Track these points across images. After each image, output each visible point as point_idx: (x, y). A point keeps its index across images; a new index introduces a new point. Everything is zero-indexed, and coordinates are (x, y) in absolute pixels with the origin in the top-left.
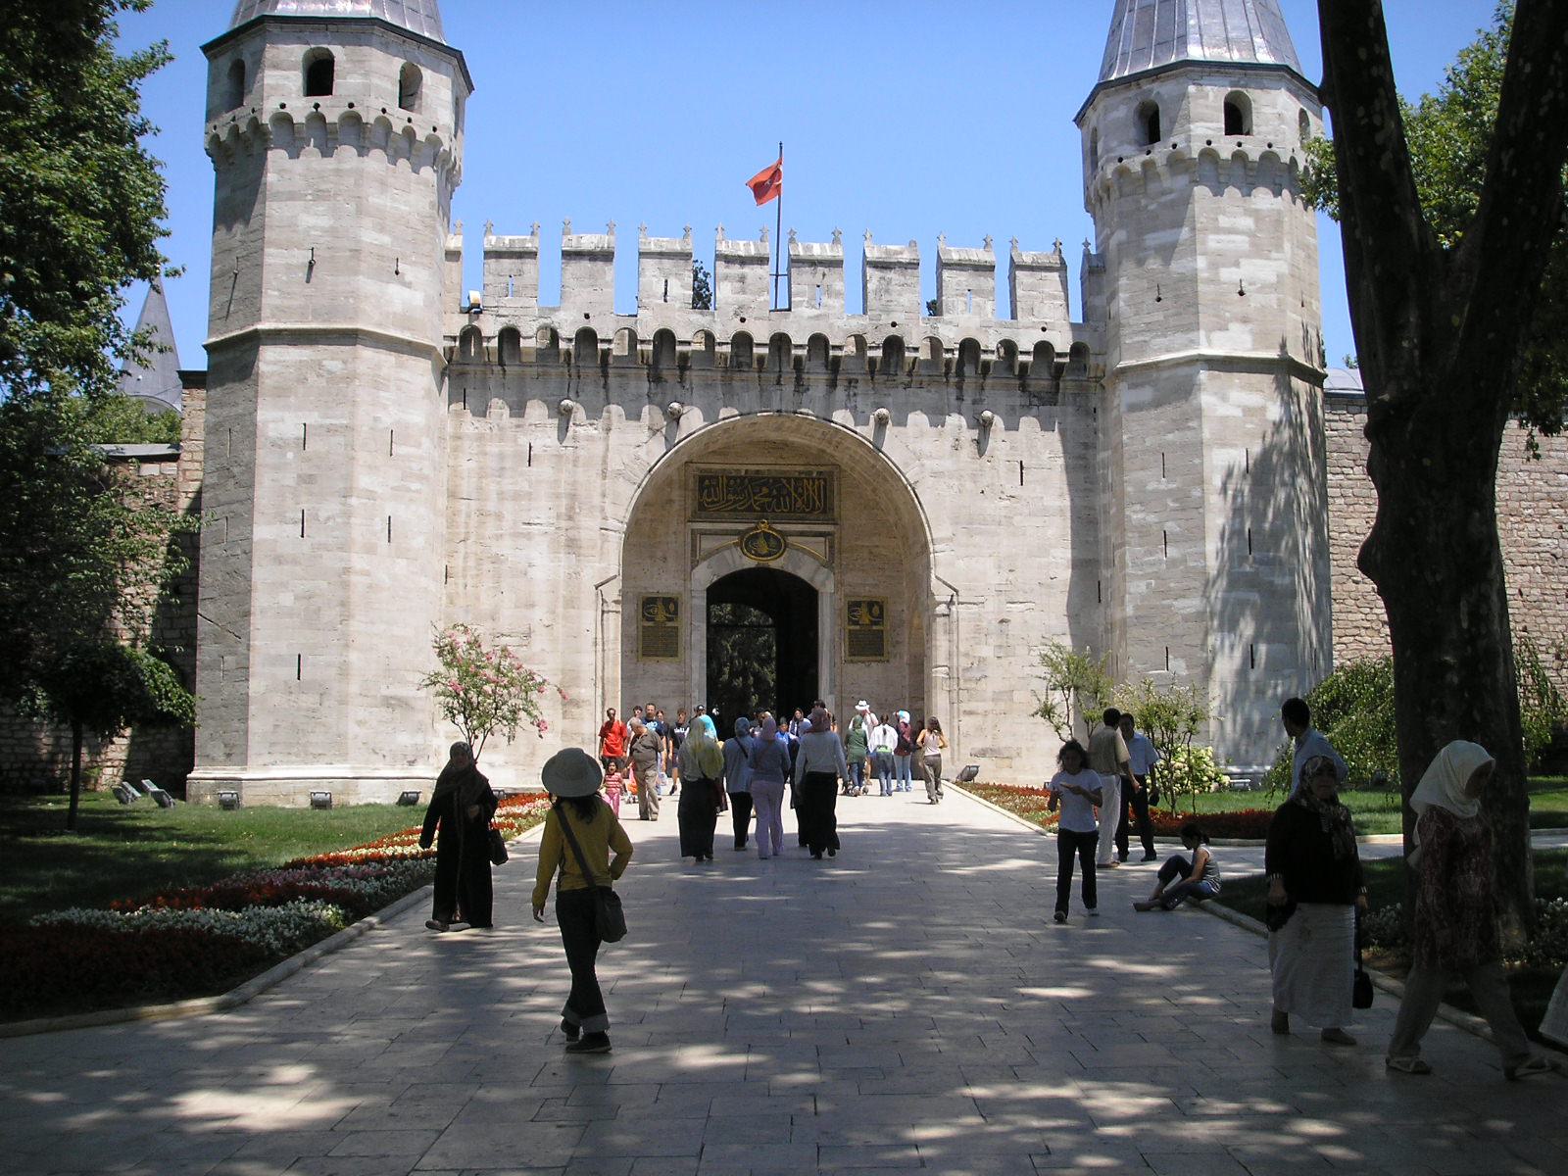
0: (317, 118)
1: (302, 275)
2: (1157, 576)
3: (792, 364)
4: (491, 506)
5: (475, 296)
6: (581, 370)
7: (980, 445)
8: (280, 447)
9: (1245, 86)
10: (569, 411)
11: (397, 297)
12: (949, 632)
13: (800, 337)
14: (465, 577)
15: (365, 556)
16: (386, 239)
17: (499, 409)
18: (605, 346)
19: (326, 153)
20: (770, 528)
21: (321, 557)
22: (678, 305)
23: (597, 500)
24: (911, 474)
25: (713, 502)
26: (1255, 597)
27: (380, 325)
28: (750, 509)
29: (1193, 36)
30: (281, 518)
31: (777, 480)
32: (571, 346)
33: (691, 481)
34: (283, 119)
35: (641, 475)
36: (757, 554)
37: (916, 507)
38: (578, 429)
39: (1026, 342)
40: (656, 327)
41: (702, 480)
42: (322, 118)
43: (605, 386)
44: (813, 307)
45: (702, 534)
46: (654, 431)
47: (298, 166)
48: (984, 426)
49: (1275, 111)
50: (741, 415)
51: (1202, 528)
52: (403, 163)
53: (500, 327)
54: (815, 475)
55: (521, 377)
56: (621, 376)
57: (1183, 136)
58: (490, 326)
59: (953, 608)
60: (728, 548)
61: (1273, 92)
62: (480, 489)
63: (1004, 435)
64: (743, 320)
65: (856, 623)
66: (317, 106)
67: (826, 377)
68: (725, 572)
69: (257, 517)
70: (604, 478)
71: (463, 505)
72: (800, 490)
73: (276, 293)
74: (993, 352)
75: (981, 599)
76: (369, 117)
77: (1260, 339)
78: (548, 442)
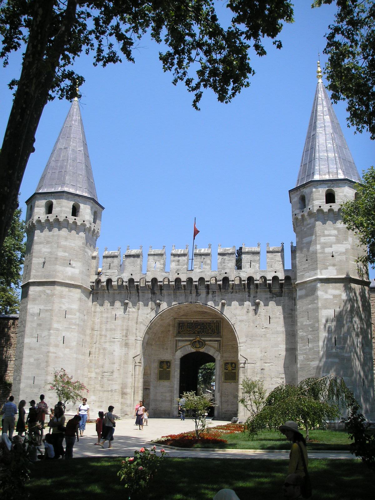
0: (48, 220)
1: (42, 266)
2: (306, 354)
3: (194, 287)
4: (103, 333)
5: (100, 269)
6: (130, 292)
7: (256, 311)
8: (33, 315)
9: (333, 187)
10: (127, 304)
11: (69, 271)
12: (244, 373)
13: (196, 279)
14: (95, 354)
15: (55, 348)
16: (67, 254)
17: (107, 304)
18: (137, 284)
19: (50, 230)
20: (200, 339)
21: (42, 348)
22: (158, 270)
23: (134, 331)
24: (232, 321)
25: (183, 331)
26: (337, 360)
27: (63, 279)
28: (194, 333)
29: (317, 172)
30: (32, 336)
31: (203, 324)
32: (127, 284)
33: (176, 325)
34: (39, 221)
35: (148, 323)
36: (196, 347)
37: (234, 332)
38: (130, 309)
39: (269, 277)
40: (152, 277)
41: (179, 324)
42: (49, 220)
43: (138, 296)
44: (200, 269)
46: (152, 309)
47: (43, 234)
48: (257, 305)
49: (344, 194)
50: (179, 304)
51: (318, 337)
52: (73, 232)
53: (106, 279)
54: (215, 322)
55: (114, 294)
56: (143, 292)
57: (311, 205)
58: (104, 279)
59: (246, 365)
60: (187, 345)
61: (342, 188)
62: (101, 328)
63: (264, 307)
64: (178, 274)
65: (227, 370)
66: (48, 217)
67: (205, 291)
68: (186, 353)
69: (26, 336)
70: (137, 324)
71: (95, 333)
72: (210, 327)
73: (34, 271)
74: (258, 280)
75: (255, 362)
76: (61, 219)
77: (339, 271)
78: (121, 313)
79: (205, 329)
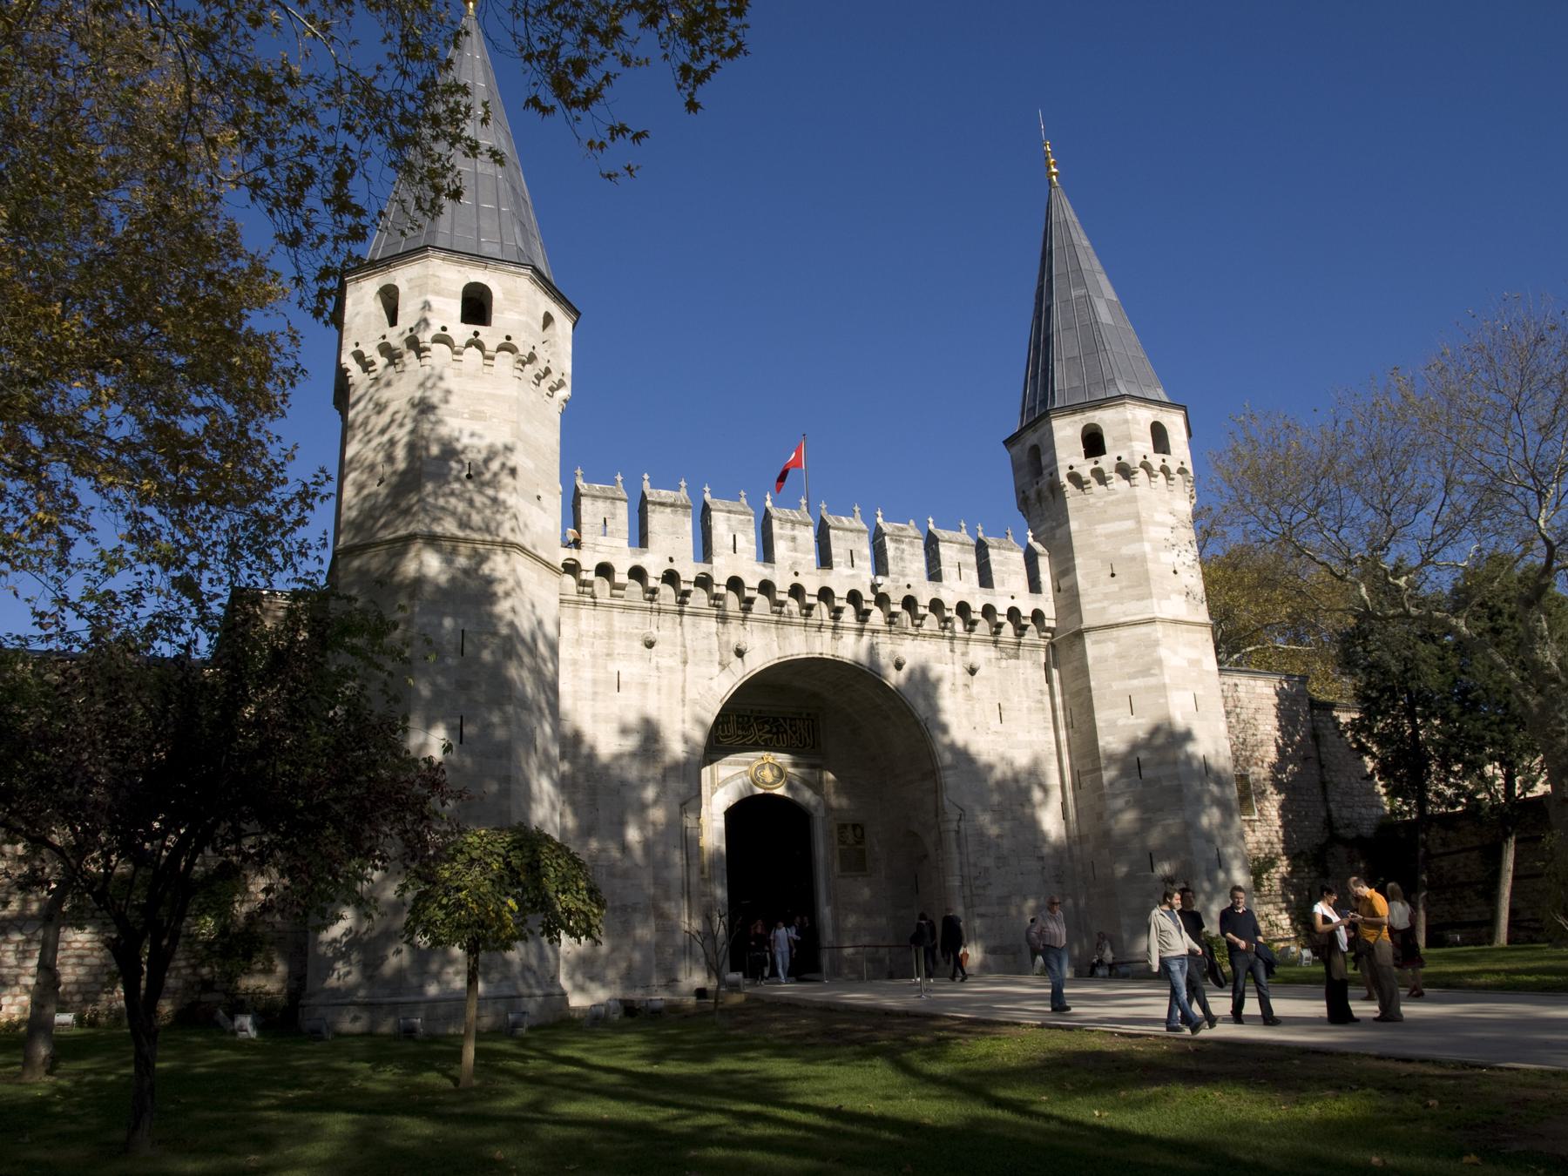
22: (745, 556)
31: (776, 720)
42: (480, 346)
65: (844, 843)
66: (476, 334)
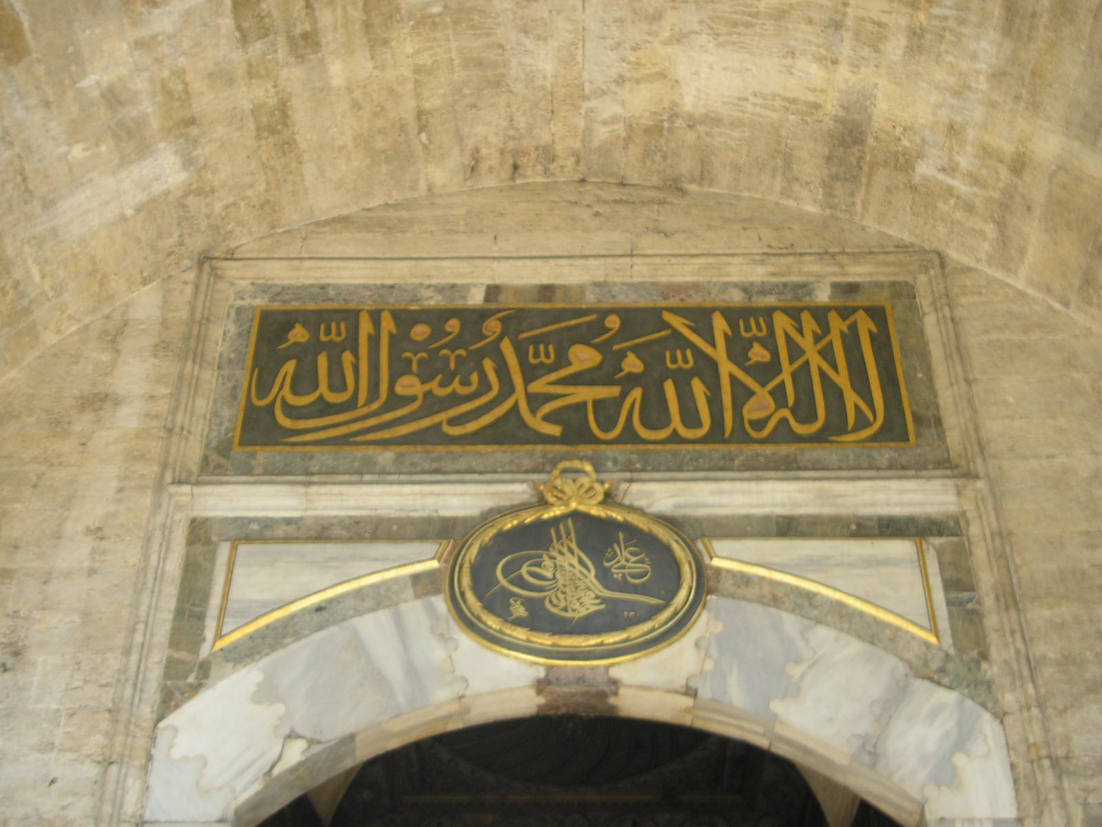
31: (639, 321)
45: (236, 541)
60: (379, 598)
79: (682, 381)
